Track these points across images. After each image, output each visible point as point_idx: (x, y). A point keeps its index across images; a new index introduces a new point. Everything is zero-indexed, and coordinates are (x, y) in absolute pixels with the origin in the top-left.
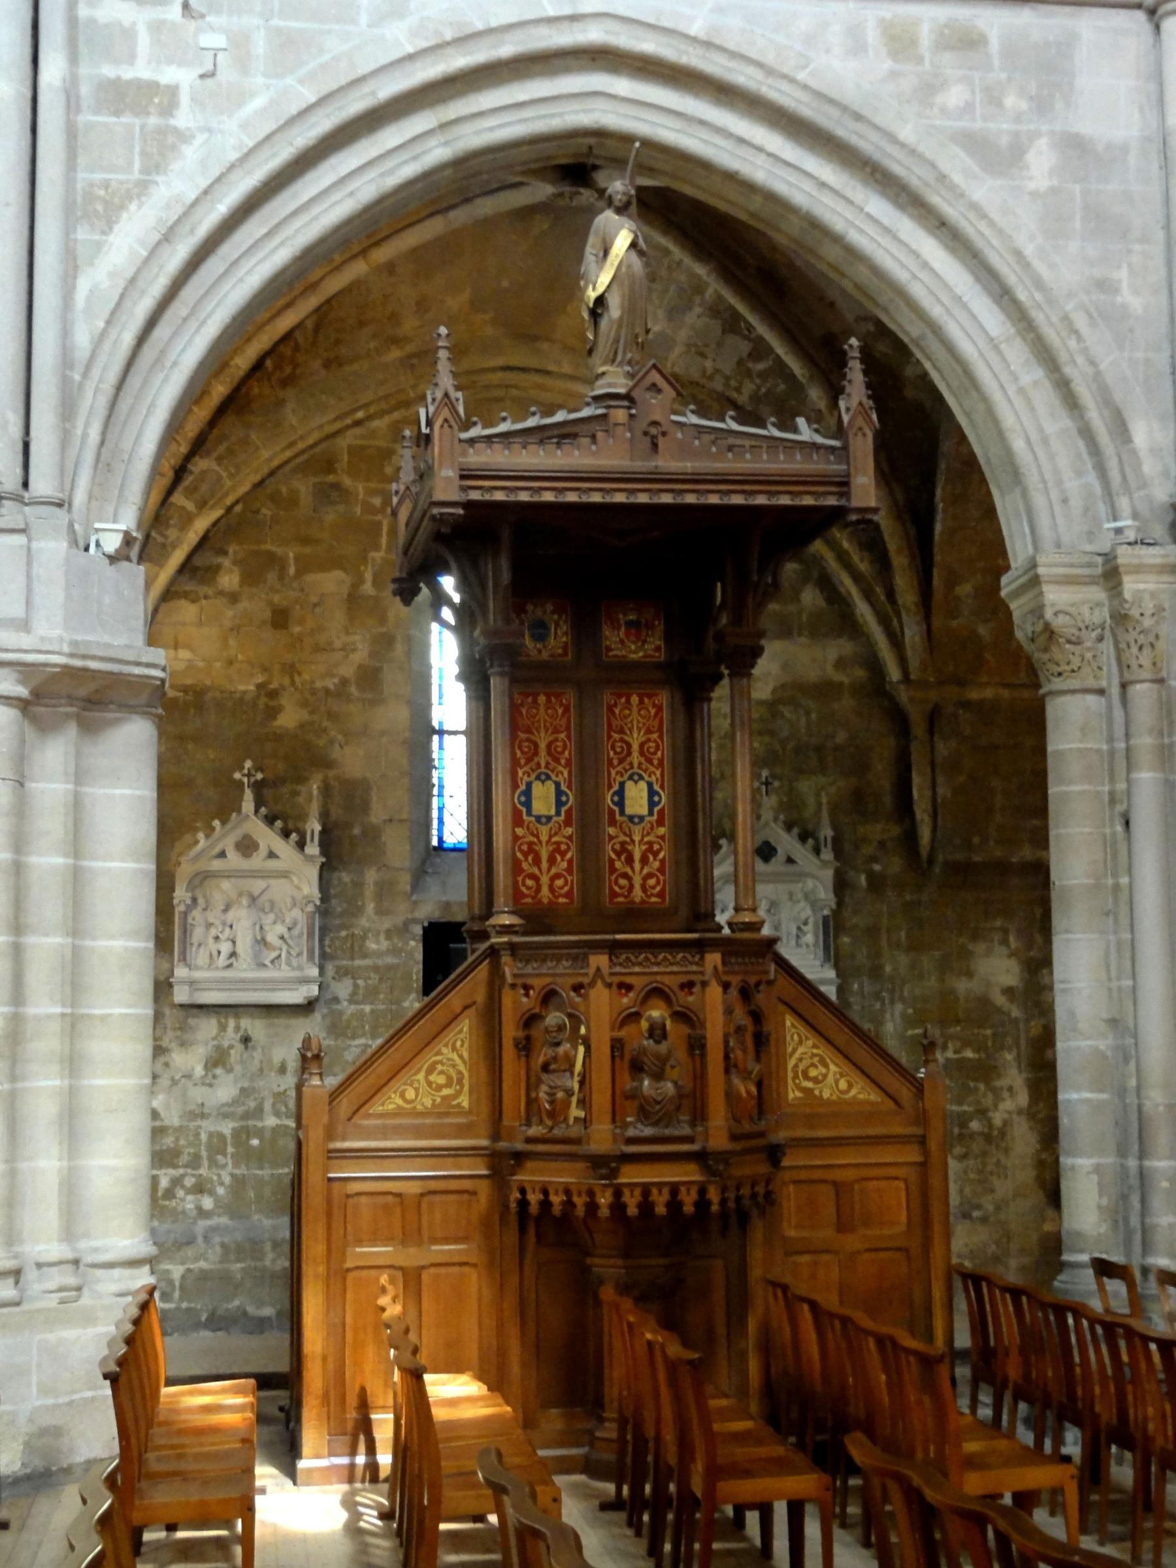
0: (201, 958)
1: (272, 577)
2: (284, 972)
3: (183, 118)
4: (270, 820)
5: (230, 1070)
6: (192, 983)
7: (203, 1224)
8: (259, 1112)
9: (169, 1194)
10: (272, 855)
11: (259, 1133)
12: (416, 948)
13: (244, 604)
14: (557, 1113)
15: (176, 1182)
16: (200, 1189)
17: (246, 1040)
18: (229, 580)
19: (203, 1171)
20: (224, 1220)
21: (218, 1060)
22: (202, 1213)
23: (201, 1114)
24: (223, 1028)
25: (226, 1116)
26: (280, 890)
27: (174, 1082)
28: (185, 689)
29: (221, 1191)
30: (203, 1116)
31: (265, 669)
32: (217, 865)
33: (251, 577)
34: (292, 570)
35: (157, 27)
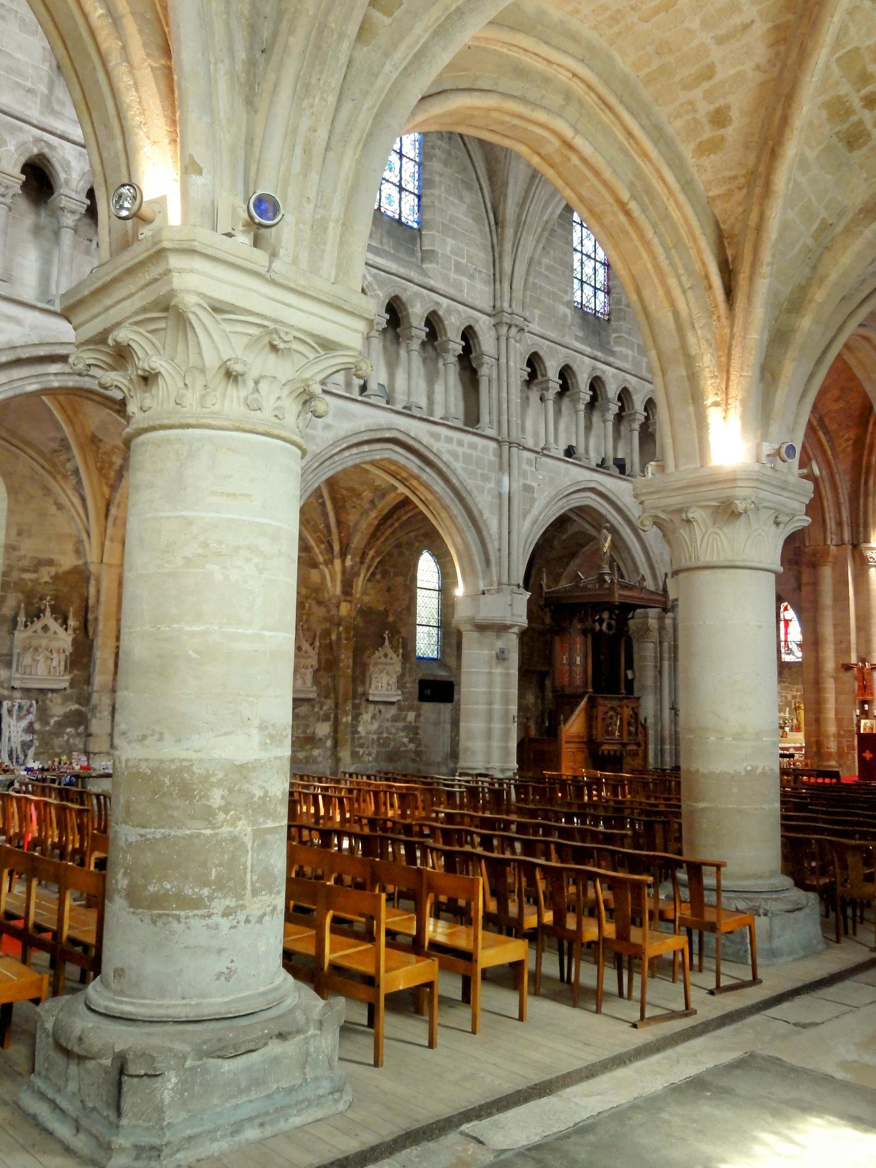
0: (373, 686)
3: (536, 495)
4: (392, 648)
6: (374, 695)
7: (370, 765)
8: (382, 733)
9: (362, 756)
11: (382, 738)
12: (417, 686)
14: (613, 733)
15: (364, 753)
16: (369, 754)
17: (380, 712)
18: (378, 577)
20: (373, 764)
21: (374, 717)
22: (370, 762)
23: (369, 733)
32: (380, 660)
35: (531, 472)
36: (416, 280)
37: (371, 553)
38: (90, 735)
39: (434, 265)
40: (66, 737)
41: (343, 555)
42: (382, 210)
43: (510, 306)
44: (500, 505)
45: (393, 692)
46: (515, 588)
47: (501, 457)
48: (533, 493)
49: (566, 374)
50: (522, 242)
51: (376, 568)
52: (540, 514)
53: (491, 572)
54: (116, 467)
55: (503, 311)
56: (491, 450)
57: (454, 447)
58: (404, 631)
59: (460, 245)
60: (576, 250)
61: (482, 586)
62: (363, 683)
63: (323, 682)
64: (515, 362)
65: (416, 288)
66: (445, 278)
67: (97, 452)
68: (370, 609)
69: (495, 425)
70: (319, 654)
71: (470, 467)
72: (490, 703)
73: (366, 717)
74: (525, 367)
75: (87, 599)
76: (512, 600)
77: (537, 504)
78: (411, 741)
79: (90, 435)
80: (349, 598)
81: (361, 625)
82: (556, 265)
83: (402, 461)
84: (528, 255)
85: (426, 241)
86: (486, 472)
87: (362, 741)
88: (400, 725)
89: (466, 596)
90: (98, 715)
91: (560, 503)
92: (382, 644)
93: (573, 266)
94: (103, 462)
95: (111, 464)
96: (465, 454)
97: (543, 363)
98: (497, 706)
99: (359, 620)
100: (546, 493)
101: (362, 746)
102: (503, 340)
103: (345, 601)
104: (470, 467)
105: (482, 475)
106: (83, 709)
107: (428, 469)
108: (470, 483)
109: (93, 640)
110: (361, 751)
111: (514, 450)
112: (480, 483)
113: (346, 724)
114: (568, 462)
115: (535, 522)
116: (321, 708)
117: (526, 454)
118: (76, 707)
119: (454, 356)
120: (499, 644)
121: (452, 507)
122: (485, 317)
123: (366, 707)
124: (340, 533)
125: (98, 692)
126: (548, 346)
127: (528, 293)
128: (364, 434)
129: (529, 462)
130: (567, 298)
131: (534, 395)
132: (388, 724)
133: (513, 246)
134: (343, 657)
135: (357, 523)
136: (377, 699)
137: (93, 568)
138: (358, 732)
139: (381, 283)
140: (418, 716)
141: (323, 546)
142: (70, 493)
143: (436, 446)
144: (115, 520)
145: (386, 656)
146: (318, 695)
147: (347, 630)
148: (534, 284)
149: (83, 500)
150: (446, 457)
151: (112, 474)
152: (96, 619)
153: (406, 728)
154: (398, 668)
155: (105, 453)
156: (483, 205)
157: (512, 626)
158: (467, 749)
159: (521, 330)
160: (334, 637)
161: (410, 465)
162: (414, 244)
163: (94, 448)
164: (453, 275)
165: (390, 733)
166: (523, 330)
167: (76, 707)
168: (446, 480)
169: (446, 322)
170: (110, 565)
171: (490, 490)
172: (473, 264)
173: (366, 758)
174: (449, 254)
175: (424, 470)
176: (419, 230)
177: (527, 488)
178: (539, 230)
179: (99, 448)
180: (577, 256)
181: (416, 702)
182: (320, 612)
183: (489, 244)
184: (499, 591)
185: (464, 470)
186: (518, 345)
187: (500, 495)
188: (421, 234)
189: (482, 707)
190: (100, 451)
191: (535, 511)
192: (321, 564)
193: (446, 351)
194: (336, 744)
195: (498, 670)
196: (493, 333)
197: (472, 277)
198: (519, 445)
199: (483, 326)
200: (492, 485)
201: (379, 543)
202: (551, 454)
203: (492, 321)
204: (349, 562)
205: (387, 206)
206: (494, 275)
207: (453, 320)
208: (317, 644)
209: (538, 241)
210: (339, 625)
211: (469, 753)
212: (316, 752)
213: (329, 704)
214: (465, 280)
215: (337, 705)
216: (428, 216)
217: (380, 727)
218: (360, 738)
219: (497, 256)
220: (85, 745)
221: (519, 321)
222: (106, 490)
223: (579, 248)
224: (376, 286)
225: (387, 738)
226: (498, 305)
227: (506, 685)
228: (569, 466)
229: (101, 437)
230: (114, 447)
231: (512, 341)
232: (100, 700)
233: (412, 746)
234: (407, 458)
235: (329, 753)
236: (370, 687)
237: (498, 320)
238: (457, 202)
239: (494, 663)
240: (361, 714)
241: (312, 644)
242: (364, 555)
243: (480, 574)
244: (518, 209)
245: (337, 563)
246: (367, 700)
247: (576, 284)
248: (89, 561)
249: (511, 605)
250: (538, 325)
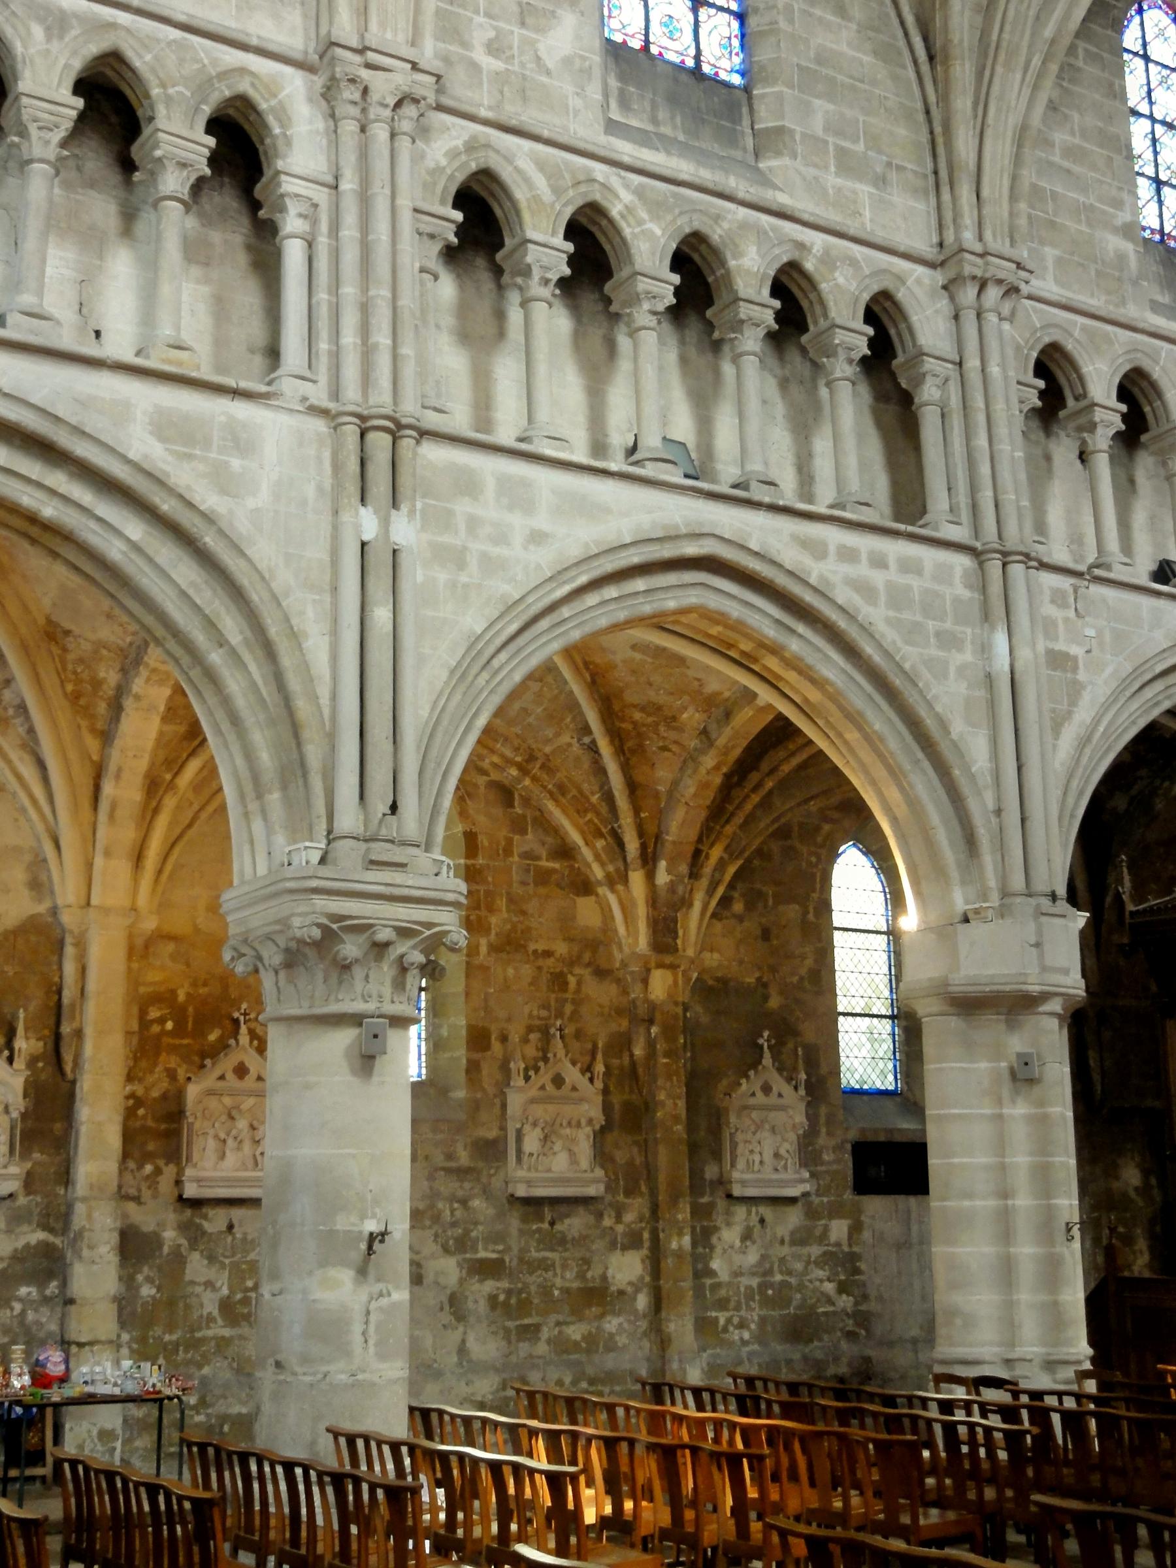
0: (741, 1164)
1: (760, 905)
2: (790, 1175)
3: (1082, 676)
4: (780, 1070)
5: (754, 1242)
6: (744, 1183)
8: (769, 1272)
10: (780, 1095)
11: (771, 1285)
12: (848, 1157)
13: (746, 924)
15: (729, 1321)
16: (742, 1325)
17: (762, 1221)
18: (738, 907)
19: (743, 1313)
20: (756, 1347)
21: (747, 1236)
22: (744, 1343)
23: (737, 1274)
24: (749, 1213)
25: (754, 1274)
26: (778, 1118)
27: (725, 1251)
28: (718, 979)
29: (753, 1326)
30: (741, 1274)
31: (760, 969)
33: (750, 906)
34: (771, 902)
35: (1067, 620)
36: (741, 195)
37: (716, 853)
38: (70, 1301)
39: (786, 161)
40: (18, 1307)
41: (648, 860)
42: (654, 50)
43: (981, 239)
44: (992, 704)
45: (790, 1175)
46: (1045, 902)
47: (984, 590)
48: (1075, 669)
49: (1136, 391)
50: (996, 89)
51: (731, 886)
52: (1097, 721)
53: (981, 868)
54: (109, 690)
55: (962, 250)
56: (958, 572)
57: (863, 570)
58: (809, 1031)
59: (849, 113)
60: (1135, 113)
61: (960, 901)
62: (717, 1155)
63: (621, 1156)
64: (1003, 366)
65: (743, 212)
66: (815, 188)
67: (63, 662)
68: (724, 982)
69: (965, 515)
70: (606, 1092)
71: (906, 615)
72: (1005, 1194)
73: (729, 1236)
74: (1030, 377)
75: (59, 992)
76: (1039, 933)
77: (1086, 697)
78: (842, 1289)
79: (42, 621)
80: (668, 959)
81: (705, 1019)
82: (1086, 145)
83: (735, 611)
84: (1014, 120)
85: (762, 110)
86: (948, 625)
87: (723, 1292)
88: (815, 1251)
89: (925, 930)
90: (85, 1253)
91: (1149, 693)
92: (756, 1063)
93: (1129, 148)
94: (78, 681)
95: (97, 684)
96: (890, 586)
97: (1076, 369)
98: (1023, 1201)
99: (699, 1009)
100: (1109, 670)
101: (722, 1304)
102: (969, 317)
103: (660, 966)
104: (906, 615)
105: (938, 634)
106: (58, 1241)
107: (801, 628)
108: (910, 655)
109: (73, 1082)
110: (722, 1318)
111: (1017, 570)
112: (934, 652)
113: (679, 1255)
114: (1158, 594)
115: (1084, 741)
116: (619, 1219)
117: (1049, 580)
118: (41, 1235)
119: (850, 361)
120: (1016, 1044)
121: (870, 714)
122: (920, 270)
123: (728, 1213)
124: (637, 811)
125: (84, 1199)
126: (1084, 329)
127: (1022, 206)
128: (632, 550)
129: (1058, 598)
130: (1123, 217)
131: (1063, 450)
132: (785, 1250)
133: (976, 104)
134: (662, 1096)
135: (675, 784)
136: (751, 1192)
137: (66, 918)
138: (712, 1273)
139: (657, 208)
140: (856, 1228)
141: (600, 844)
142: (14, 755)
143: (816, 570)
144: (113, 807)
145: (767, 1089)
146: (608, 1188)
147: (668, 1032)
148: (1036, 190)
149: (41, 765)
150: (843, 595)
151: (102, 708)
152: (79, 1034)
153: (828, 1259)
154: (800, 1118)
155: (81, 661)
156: (895, 21)
157: (1045, 997)
158: (953, 1312)
159: (1012, 291)
160: (638, 1052)
161: (754, 620)
162: (736, 119)
163: (56, 650)
164: (832, 180)
165: (790, 1273)
166: (1017, 290)
167: (38, 1236)
168: (850, 651)
169: (824, 286)
170: (106, 911)
171: (962, 670)
172: (880, 152)
173: (735, 1335)
174: (820, 132)
175: (792, 631)
176: (747, 89)
177: (1058, 660)
178: (1036, 61)
179: (65, 650)
180: (1139, 129)
181: (848, 1195)
182: (601, 993)
183: (919, 105)
184: (1003, 911)
185: (888, 621)
186: (1006, 326)
187: (989, 679)
188: (750, 98)
189: (986, 1204)
190: (71, 657)
191: (1083, 714)
192: (600, 883)
193: (831, 352)
194: (657, 1303)
195: (1019, 1110)
196: (943, 303)
197: (881, 182)
198: (1027, 556)
199: (917, 291)
200: (967, 656)
201: (729, 829)
202: (1111, 575)
203: (939, 277)
204: (662, 877)
205: (665, 42)
206: (936, 173)
207: (841, 280)
208: (600, 1068)
209: (1036, 87)
210: (651, 1022)
211: (958, 1322)
212: (612, 1324)
213: (635, 1210)
214: (864, 189)
215: (655, 1209)
216: (764, 54)
217: (764, 1257)
218: (716, 1287)
219: (938, 129)
220: (62, 1325)
221: (1005, 270)
222: (93, 744)
223: (1144, 108)
224: (644, 215)
225: (784, 1284)
226: (950, 237)
227: (1043, 1146)
228: (1162, 603)
229: (67, 625)
230: (100, 645)
231: (992, 318)
232: (89, 1217)
233: (845, 1302)
234: (747, 604)
235: (643, 1325)
236: (733, 1165)
237: (951, 272)
238: (830, 17)
239: (1006, 1090)
240: (716, 1229)
241: (588, 1069)
242: (697, 856)
243: (954, 874)
244: (979, 19)
245: (637, 878)
246: (729, 1196)
247: (1145, 189)
248: (60, 902)
249: (1038, 945)
250: (1057, 281)
